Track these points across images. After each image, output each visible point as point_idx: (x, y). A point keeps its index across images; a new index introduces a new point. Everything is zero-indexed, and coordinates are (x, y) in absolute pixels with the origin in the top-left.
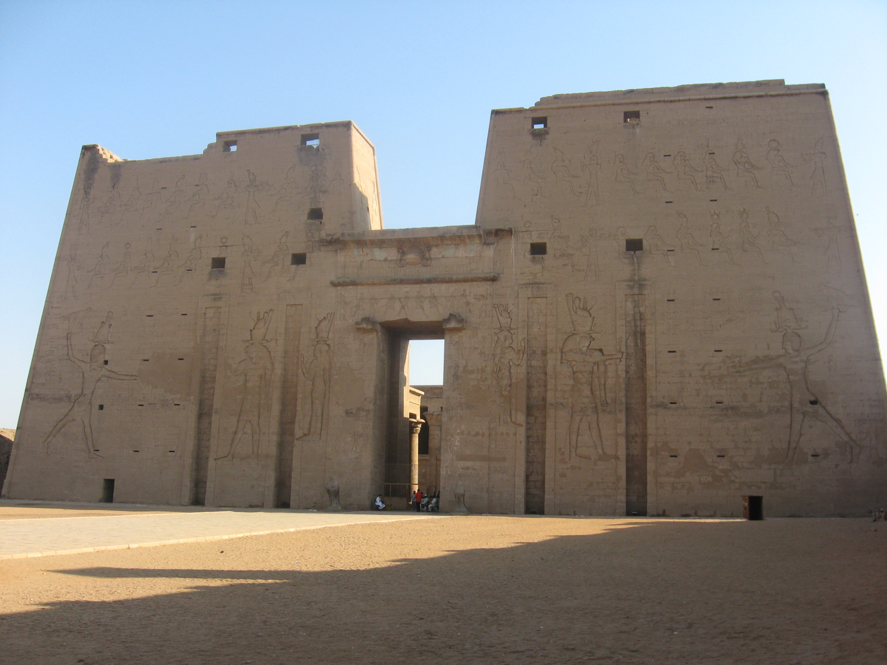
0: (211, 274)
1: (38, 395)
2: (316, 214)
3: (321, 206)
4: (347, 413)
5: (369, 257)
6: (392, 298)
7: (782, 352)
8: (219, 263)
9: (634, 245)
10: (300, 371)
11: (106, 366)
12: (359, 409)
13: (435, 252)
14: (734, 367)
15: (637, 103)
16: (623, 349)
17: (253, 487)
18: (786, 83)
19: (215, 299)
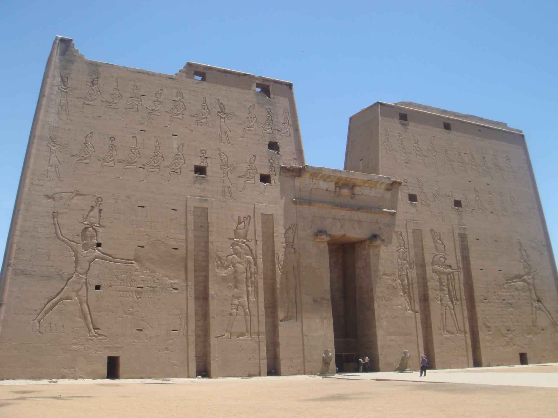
0: (196, 180)
1: (22, 271)
2: (273, 146)
3: (277, 141)
4: (315, 301)
5: (316, 186)
6: (334, 218)
7: (524, 273)
8: (200, 170)
9: (458, 204)
10: (277, 266)
11: (99, 248)
12: (322, 298)
13: (357, 190)
14: (507, 280)
15: (449, 119)
16: (461, 266)
17: (250, 359)
18: (509, 126)
19: (201, 201)
